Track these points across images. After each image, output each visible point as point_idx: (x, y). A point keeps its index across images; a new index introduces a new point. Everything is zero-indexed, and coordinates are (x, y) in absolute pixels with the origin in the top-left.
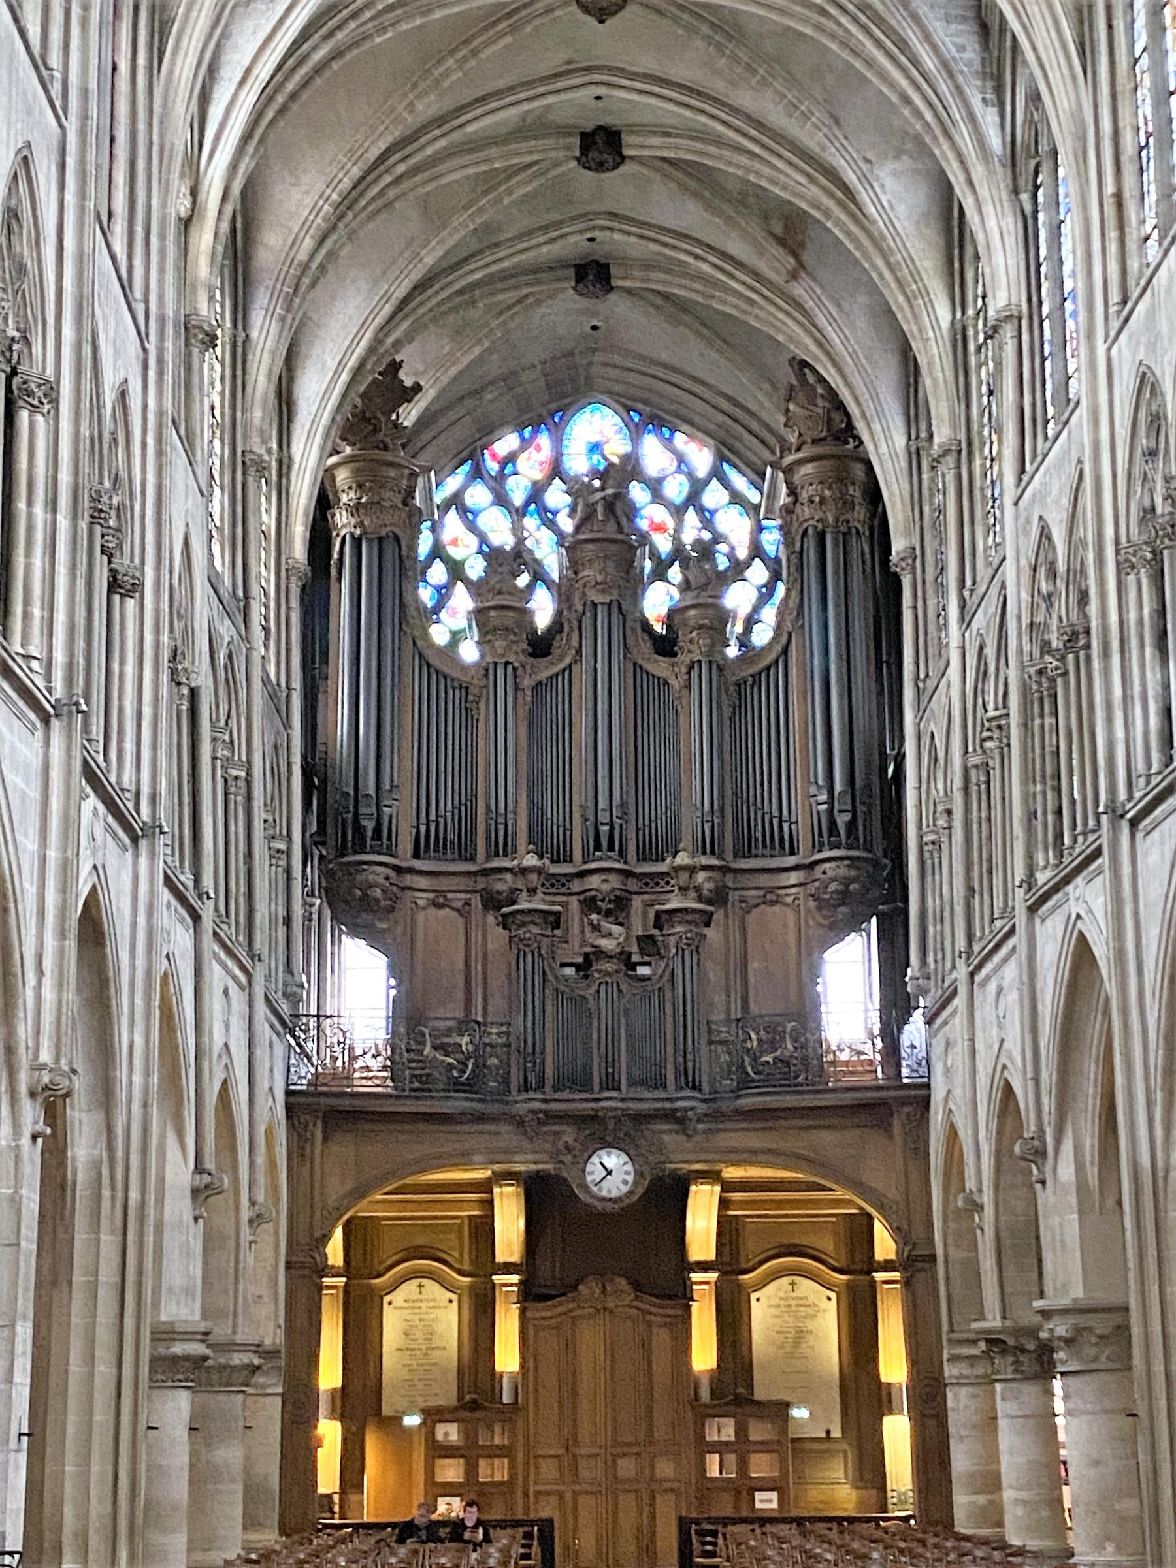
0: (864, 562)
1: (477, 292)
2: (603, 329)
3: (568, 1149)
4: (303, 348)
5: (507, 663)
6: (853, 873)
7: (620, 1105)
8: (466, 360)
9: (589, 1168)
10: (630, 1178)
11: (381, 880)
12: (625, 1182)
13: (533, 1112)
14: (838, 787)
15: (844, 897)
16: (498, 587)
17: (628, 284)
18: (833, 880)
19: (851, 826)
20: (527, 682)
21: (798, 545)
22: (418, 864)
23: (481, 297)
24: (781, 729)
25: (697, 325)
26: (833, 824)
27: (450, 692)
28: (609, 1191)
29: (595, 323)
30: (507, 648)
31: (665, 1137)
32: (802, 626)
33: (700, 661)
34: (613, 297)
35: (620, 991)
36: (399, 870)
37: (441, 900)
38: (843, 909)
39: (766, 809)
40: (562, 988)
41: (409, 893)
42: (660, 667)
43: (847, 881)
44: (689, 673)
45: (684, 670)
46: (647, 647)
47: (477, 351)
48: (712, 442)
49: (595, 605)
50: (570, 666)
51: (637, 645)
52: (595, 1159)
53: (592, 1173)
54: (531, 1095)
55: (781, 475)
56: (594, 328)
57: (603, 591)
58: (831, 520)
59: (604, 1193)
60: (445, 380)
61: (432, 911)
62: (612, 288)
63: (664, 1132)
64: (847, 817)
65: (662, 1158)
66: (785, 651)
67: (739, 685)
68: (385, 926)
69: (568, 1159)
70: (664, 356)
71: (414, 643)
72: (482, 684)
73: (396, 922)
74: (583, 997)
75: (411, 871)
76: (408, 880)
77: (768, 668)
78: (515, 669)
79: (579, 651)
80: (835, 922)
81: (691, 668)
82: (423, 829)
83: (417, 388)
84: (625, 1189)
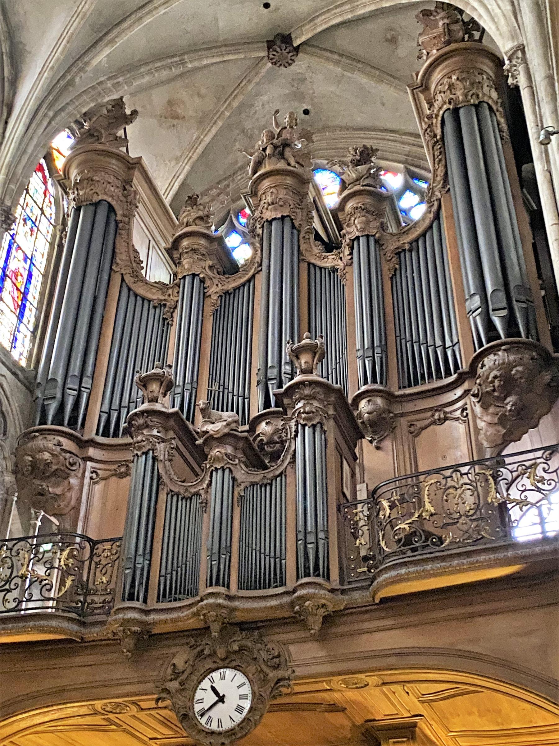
0: (500, 131)
1: (186, 57)
2: (312, 114)
3: (177, 675)
4: (24, 73)
5: (194, 275)
6: (512, 358)
7: (220, 601)
8: (208, 139)
9: (199, 695)
10: (247, 704)
11: (50, 445)
12: (239, 709)
13: (126, 622)
14: (490, 289)
15: (508, 383)
16: (185, 220)
17: (304, 39)
18: (491, 369)
19: (510, 322)
20: (214, 290)
21: (438, 131)
22: (101, 439)
23: (191, 62)
24: (438, 275)
25: (368, 69)
26: (490, 326)
27: (152, 311)
28: (220, 721)
29: (305, 107)
30: (191, 264)
31: (292, 648)
32: (449, 190)
33: (358, 238)
34: (301, 64)
35: (234, 479)
36: (83, 444)
37: (123, 469)
38: (511, 399)
39: (430, 342)
40: (176, 490)
41: (89, 464)
42: (330, 261)
43: (506, 367)
44: (351, 254)
45: (347, 252)
46: (317, 248)
47: (214, 131)
48: (402, 166)
49: (270, 222)
50: (253, 276)
51: (310, 251)
52: (206, 684)
53: (201, 701)
54: (128, 604)
55: (422, 97)
56: (306, 112)
57: (275, 210)
58: (461, 98)
59: (214, 726)
60: (195, 157)
61: (114, 479)
62: (297, 50)
63: (294, 642)
64: (504, 313)
65: (286, 674)
66: (437, 216)
67: (398, 254)
68: (58, 491)
69: (174, 685)
70: (360, 120)
71: (123, 280)
72: (176, 299)
73: (70, 489)
74: (197, 494)
75: (92, 443)
76: (92, 452)
77: (424, 235)
78: (202, 281)
79: (260, 265)
80: (504, 415)
81: (352, 248)
82: (115, 415)
83: (134, 113)
84: (239, 718)
